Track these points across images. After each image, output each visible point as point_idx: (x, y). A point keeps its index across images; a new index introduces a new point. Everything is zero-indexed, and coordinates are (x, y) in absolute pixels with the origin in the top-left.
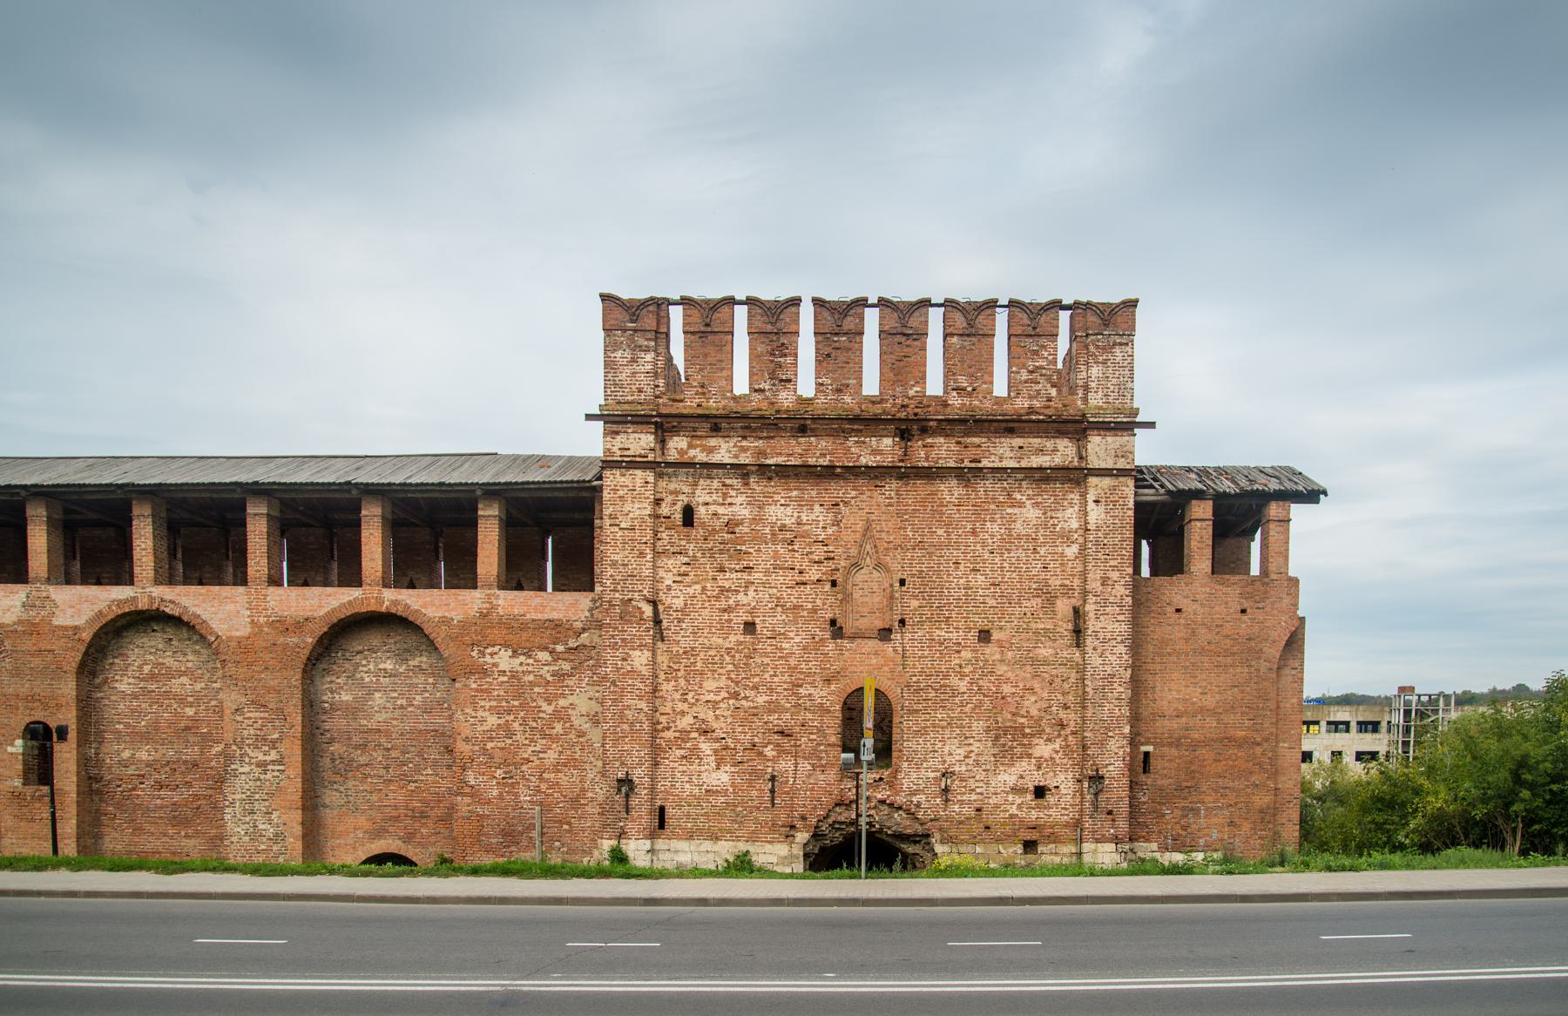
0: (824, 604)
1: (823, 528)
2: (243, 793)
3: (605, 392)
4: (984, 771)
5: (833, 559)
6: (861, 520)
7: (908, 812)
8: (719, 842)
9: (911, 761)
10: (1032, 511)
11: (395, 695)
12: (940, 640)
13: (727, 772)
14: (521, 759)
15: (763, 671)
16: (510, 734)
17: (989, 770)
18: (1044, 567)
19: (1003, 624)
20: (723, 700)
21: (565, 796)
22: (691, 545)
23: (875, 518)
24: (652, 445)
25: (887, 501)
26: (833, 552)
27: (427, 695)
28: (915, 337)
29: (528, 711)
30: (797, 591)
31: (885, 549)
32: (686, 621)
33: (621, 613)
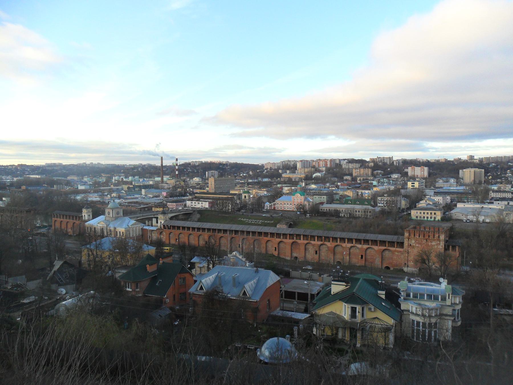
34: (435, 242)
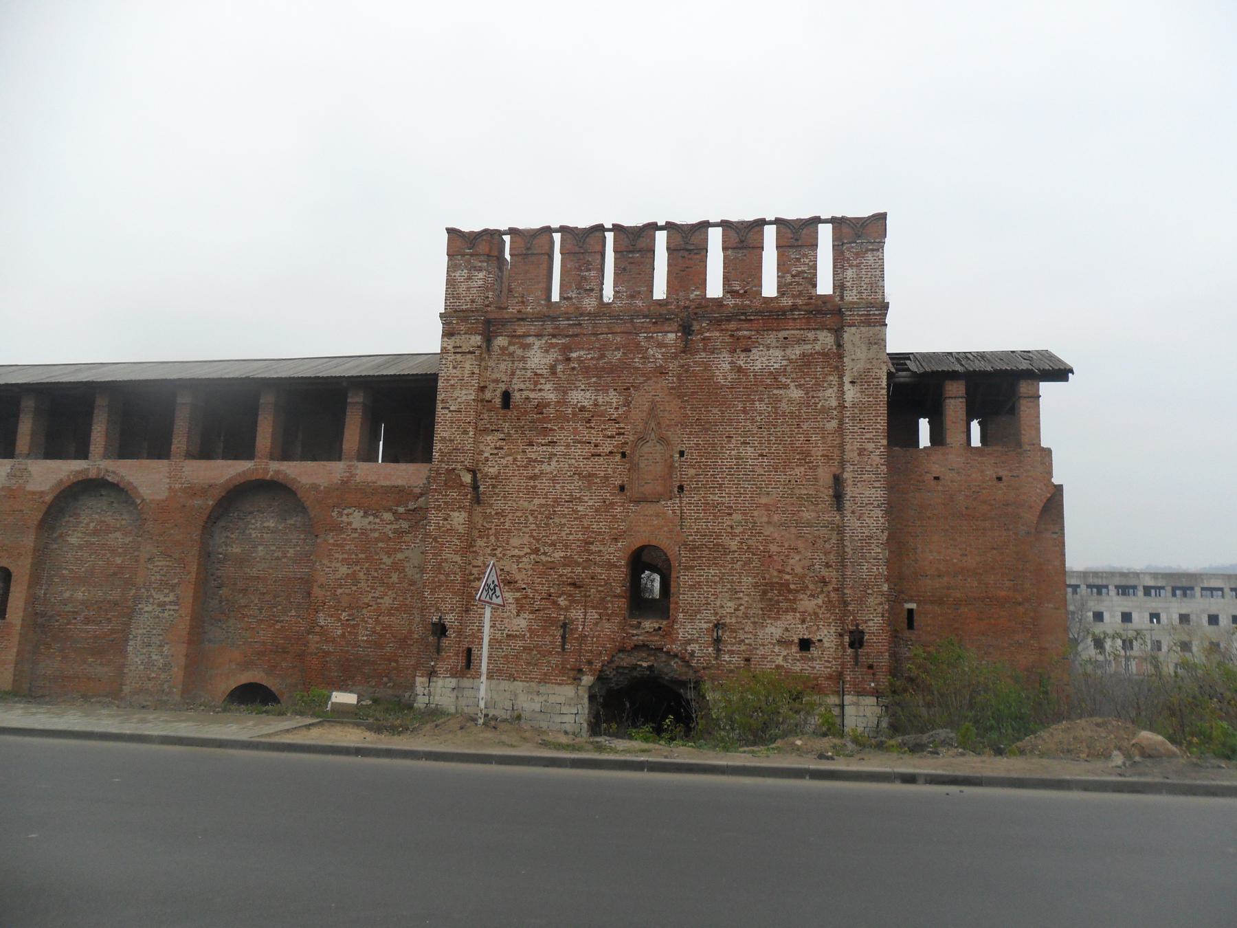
0: (614, 472)
1: (615, 408)
2: (144, 628)
3: (446, 303)
5: (623, 434)
6: (648, 402)
7: (683, 659)
8: (516, 682)
9: (685, 612)
10: (795, 392)
11: (274, 548)
13: (525, 619)
14: (363, 603)
16: (356, 582)
17: (757, 623)
18: (806, 440)
20: (526, 554)
21: (395, 637)
22: (507, 424)
23: (659, 400)
24: (479, 344)
25: (670, 385)
26: (624, 428)
27: (298, 549)
28: (695, 251)
29: (371, 563)
30: (592, 462)
31: (668, 425)
32: (499, 487)
33: (446, 480)
34: (785, 344)
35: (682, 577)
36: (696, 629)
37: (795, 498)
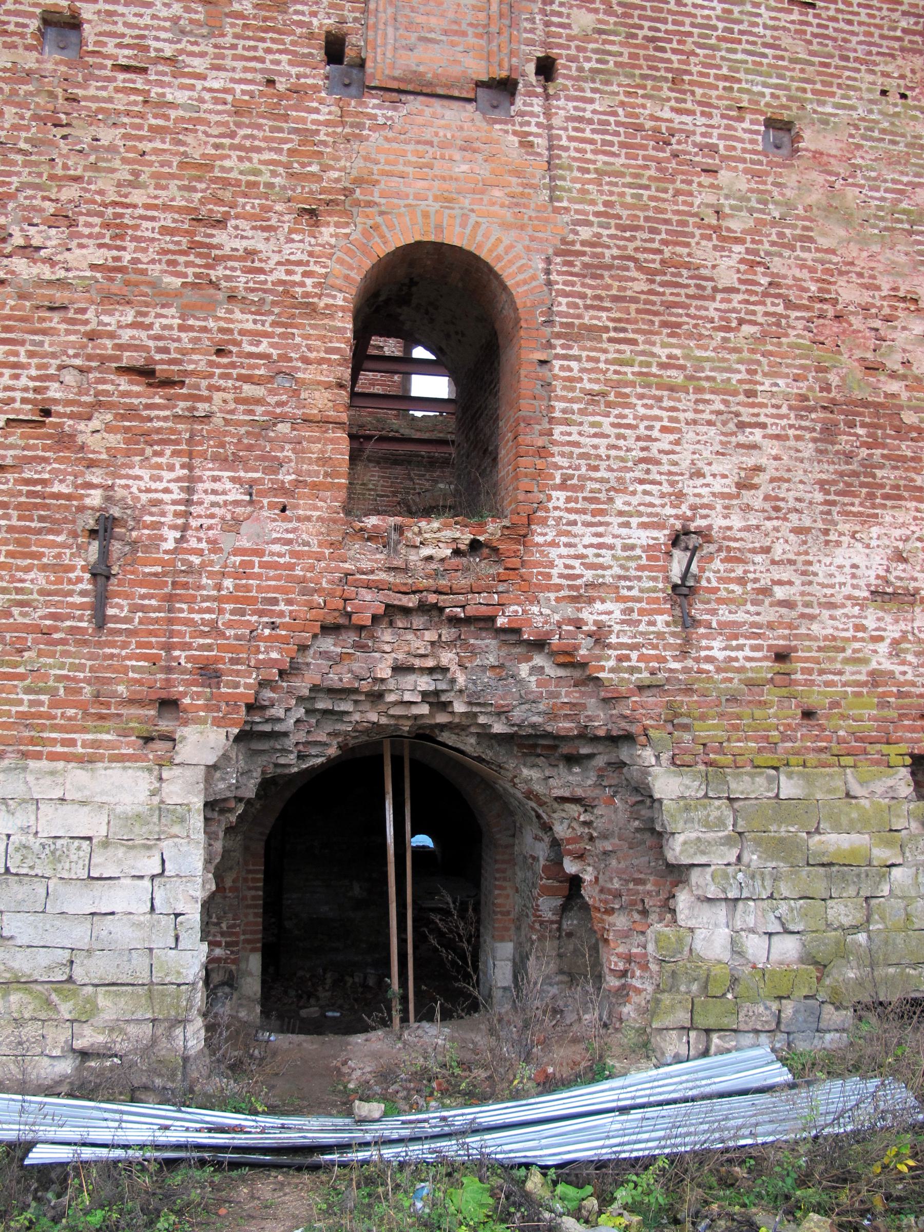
4: (797, 531)
9: (574, 488)
12: (656, 130)
15: (94, 167)
17: (807, 530)
19: (829, 109)
35: (557, 363)
36: (611, 547)
37: (901, 147)
